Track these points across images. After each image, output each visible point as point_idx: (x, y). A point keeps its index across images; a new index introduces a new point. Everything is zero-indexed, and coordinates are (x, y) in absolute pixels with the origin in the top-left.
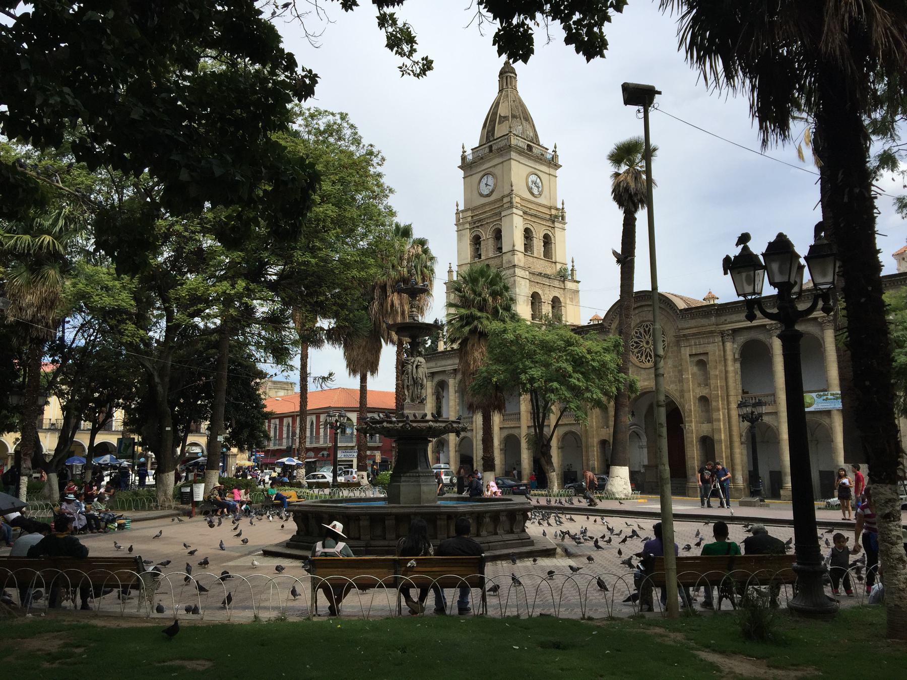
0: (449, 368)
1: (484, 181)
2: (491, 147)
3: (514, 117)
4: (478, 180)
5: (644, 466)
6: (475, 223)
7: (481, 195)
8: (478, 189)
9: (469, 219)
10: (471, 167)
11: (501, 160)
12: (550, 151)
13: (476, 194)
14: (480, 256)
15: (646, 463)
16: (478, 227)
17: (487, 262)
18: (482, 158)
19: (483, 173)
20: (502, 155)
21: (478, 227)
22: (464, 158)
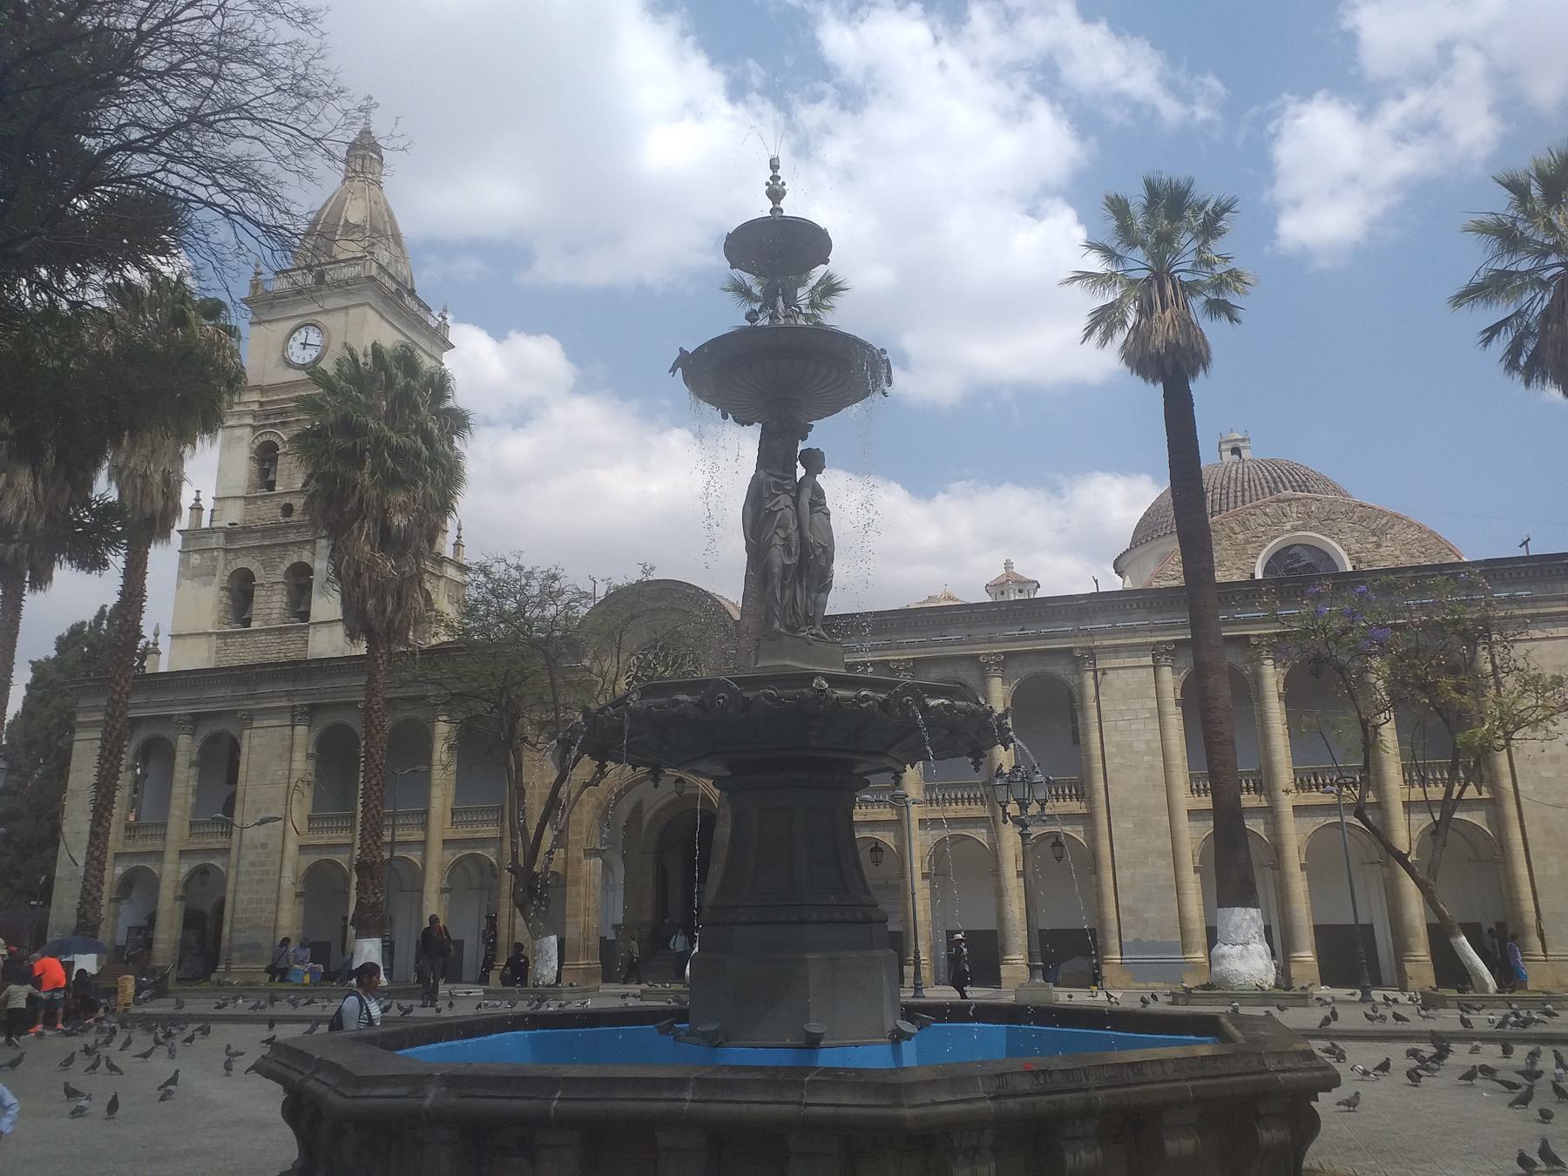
0: (183, 710)
1: (300, 337)
2: (320, 279)
3: (374, 229)
4: (287, 332)
5: (616, 927)
6: (267, 417)
7: (289, 364)
8: (285, 348)
9: (255, 407)
10: (272, 306)
11: (343, 302)
12: (436, 314)
13: (275, 356)
14: (271, 486)
15: (619, 920)
16: (274, 425)
17: (287, 500)
18: (299, 292)
19: (293, 323)
20: (348, 293)
21: (274, 425)
22: (255, 286)
